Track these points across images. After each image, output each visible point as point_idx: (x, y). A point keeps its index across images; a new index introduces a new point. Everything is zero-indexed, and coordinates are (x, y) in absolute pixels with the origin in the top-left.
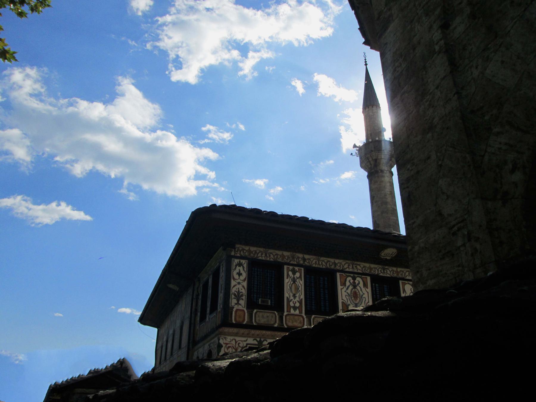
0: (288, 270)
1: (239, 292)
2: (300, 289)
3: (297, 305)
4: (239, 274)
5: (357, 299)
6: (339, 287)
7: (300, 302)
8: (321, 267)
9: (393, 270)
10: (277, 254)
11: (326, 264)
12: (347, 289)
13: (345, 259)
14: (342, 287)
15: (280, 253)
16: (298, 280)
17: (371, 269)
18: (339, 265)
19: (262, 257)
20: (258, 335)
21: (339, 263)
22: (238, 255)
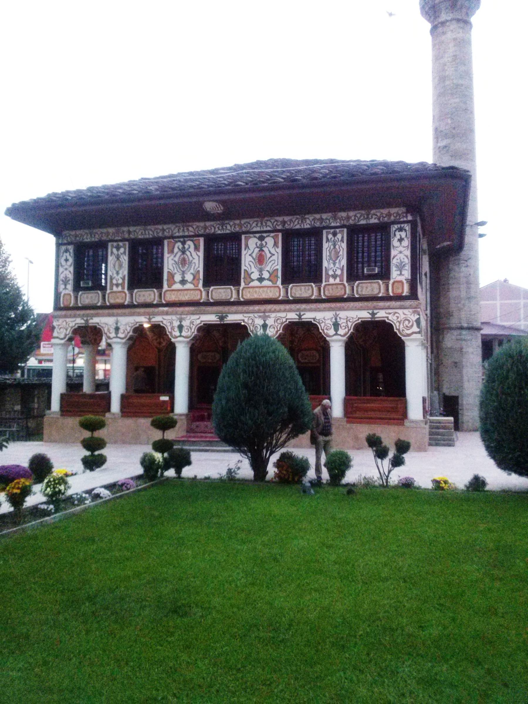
0: (112, 246)
1: (66, 278)
2: (124, 265)
3: (120, 281)
4: (67, 260)
5: (185, 265)
6: (166, 255)
7: (123, 279)
8: (148, 236)
9: (235, 224)
10: (102, 233)
11: (154, 233)
12: (175, 256)
13: (173, 222)
14: (169, 255)
15: (105, 230)
16: (122, 256)
17: (205, 228)
18: (167, 231)
19: (87, 239)
20: (83, 315)
21: (167, 229)
22: (65, 242)
